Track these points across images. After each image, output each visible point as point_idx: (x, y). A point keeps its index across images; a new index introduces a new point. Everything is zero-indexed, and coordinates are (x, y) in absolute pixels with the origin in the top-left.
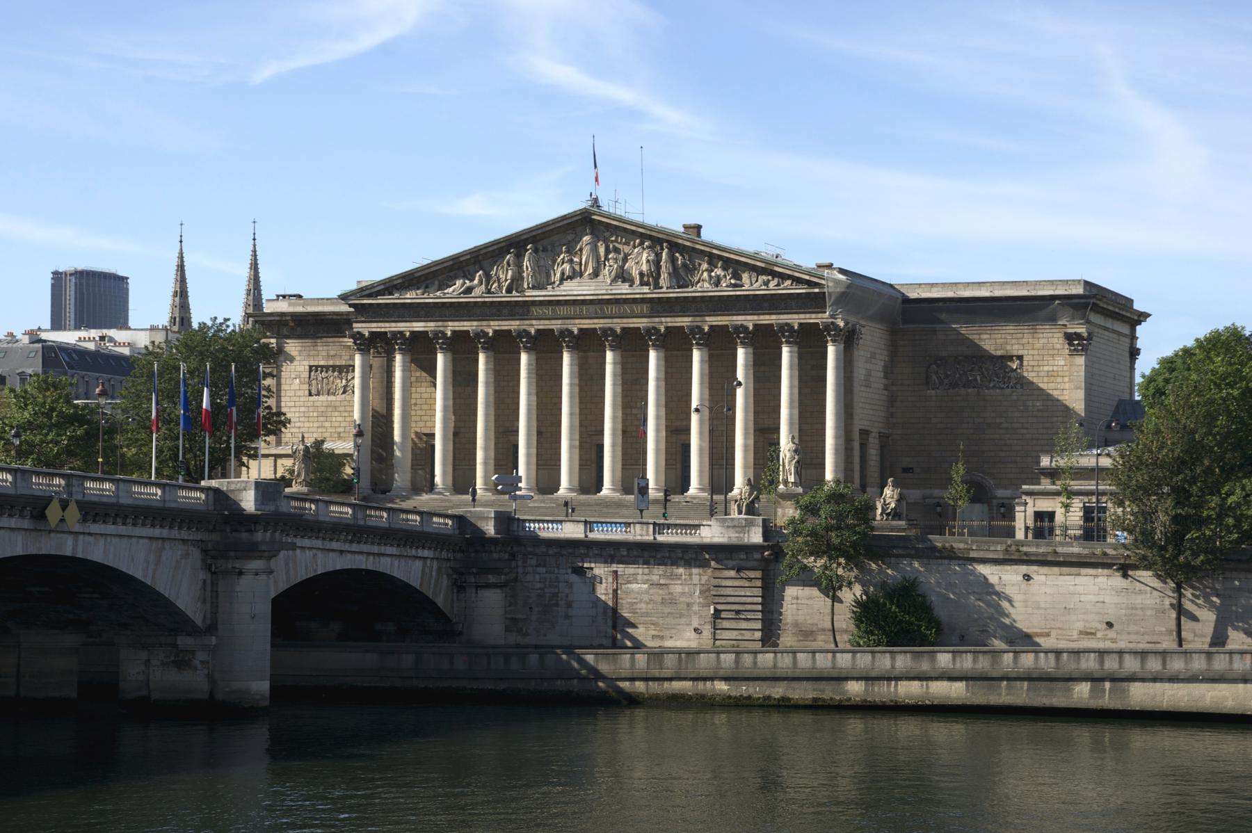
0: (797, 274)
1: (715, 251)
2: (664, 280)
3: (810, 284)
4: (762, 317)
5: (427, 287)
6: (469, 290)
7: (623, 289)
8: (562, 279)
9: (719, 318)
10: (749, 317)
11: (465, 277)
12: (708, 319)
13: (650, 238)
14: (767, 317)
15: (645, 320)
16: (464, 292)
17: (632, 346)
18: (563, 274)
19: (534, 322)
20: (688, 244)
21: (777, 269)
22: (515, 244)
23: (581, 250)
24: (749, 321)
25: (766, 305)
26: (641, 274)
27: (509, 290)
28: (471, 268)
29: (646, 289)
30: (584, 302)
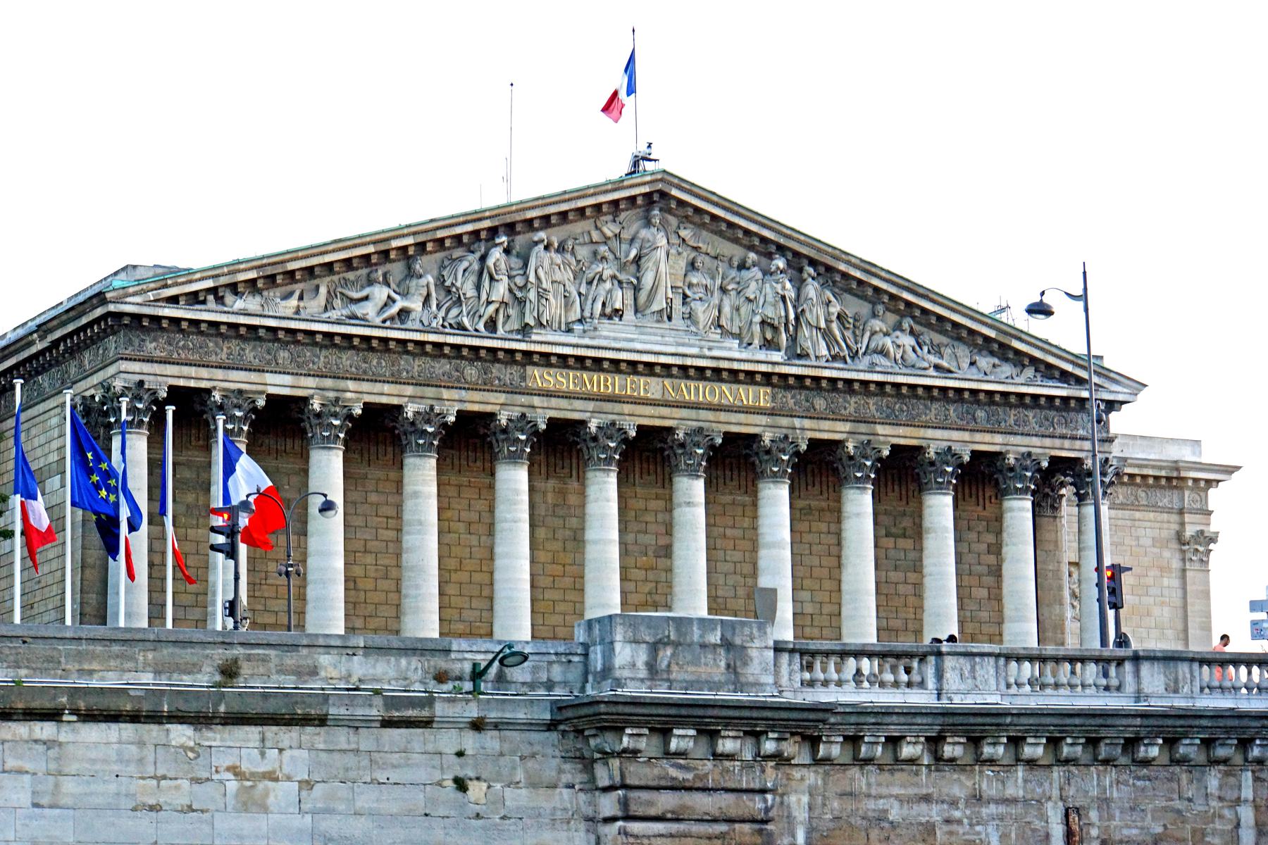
0: (1051, 360)
3: (1065, 377)
4: (978, 437)
6: (404, 313)
7: (731, 352)
8: (603, 315)
9: (901, 431)
10: (956, 435)
12: (880, 429)
13: (781, 249)
14: (987, 437)
15: (764, 420)
16: (392, 318)
18: (604, 304)
19: (536, 401)
20: (858, 274)
21: (1016, 344)
22: (510, 228)
23: (637, 260)
24: (966, 443)
25: (980, 414)
26: (763, 323)
28: (397, 269)
29: (777, 356)
30: (649, 369)
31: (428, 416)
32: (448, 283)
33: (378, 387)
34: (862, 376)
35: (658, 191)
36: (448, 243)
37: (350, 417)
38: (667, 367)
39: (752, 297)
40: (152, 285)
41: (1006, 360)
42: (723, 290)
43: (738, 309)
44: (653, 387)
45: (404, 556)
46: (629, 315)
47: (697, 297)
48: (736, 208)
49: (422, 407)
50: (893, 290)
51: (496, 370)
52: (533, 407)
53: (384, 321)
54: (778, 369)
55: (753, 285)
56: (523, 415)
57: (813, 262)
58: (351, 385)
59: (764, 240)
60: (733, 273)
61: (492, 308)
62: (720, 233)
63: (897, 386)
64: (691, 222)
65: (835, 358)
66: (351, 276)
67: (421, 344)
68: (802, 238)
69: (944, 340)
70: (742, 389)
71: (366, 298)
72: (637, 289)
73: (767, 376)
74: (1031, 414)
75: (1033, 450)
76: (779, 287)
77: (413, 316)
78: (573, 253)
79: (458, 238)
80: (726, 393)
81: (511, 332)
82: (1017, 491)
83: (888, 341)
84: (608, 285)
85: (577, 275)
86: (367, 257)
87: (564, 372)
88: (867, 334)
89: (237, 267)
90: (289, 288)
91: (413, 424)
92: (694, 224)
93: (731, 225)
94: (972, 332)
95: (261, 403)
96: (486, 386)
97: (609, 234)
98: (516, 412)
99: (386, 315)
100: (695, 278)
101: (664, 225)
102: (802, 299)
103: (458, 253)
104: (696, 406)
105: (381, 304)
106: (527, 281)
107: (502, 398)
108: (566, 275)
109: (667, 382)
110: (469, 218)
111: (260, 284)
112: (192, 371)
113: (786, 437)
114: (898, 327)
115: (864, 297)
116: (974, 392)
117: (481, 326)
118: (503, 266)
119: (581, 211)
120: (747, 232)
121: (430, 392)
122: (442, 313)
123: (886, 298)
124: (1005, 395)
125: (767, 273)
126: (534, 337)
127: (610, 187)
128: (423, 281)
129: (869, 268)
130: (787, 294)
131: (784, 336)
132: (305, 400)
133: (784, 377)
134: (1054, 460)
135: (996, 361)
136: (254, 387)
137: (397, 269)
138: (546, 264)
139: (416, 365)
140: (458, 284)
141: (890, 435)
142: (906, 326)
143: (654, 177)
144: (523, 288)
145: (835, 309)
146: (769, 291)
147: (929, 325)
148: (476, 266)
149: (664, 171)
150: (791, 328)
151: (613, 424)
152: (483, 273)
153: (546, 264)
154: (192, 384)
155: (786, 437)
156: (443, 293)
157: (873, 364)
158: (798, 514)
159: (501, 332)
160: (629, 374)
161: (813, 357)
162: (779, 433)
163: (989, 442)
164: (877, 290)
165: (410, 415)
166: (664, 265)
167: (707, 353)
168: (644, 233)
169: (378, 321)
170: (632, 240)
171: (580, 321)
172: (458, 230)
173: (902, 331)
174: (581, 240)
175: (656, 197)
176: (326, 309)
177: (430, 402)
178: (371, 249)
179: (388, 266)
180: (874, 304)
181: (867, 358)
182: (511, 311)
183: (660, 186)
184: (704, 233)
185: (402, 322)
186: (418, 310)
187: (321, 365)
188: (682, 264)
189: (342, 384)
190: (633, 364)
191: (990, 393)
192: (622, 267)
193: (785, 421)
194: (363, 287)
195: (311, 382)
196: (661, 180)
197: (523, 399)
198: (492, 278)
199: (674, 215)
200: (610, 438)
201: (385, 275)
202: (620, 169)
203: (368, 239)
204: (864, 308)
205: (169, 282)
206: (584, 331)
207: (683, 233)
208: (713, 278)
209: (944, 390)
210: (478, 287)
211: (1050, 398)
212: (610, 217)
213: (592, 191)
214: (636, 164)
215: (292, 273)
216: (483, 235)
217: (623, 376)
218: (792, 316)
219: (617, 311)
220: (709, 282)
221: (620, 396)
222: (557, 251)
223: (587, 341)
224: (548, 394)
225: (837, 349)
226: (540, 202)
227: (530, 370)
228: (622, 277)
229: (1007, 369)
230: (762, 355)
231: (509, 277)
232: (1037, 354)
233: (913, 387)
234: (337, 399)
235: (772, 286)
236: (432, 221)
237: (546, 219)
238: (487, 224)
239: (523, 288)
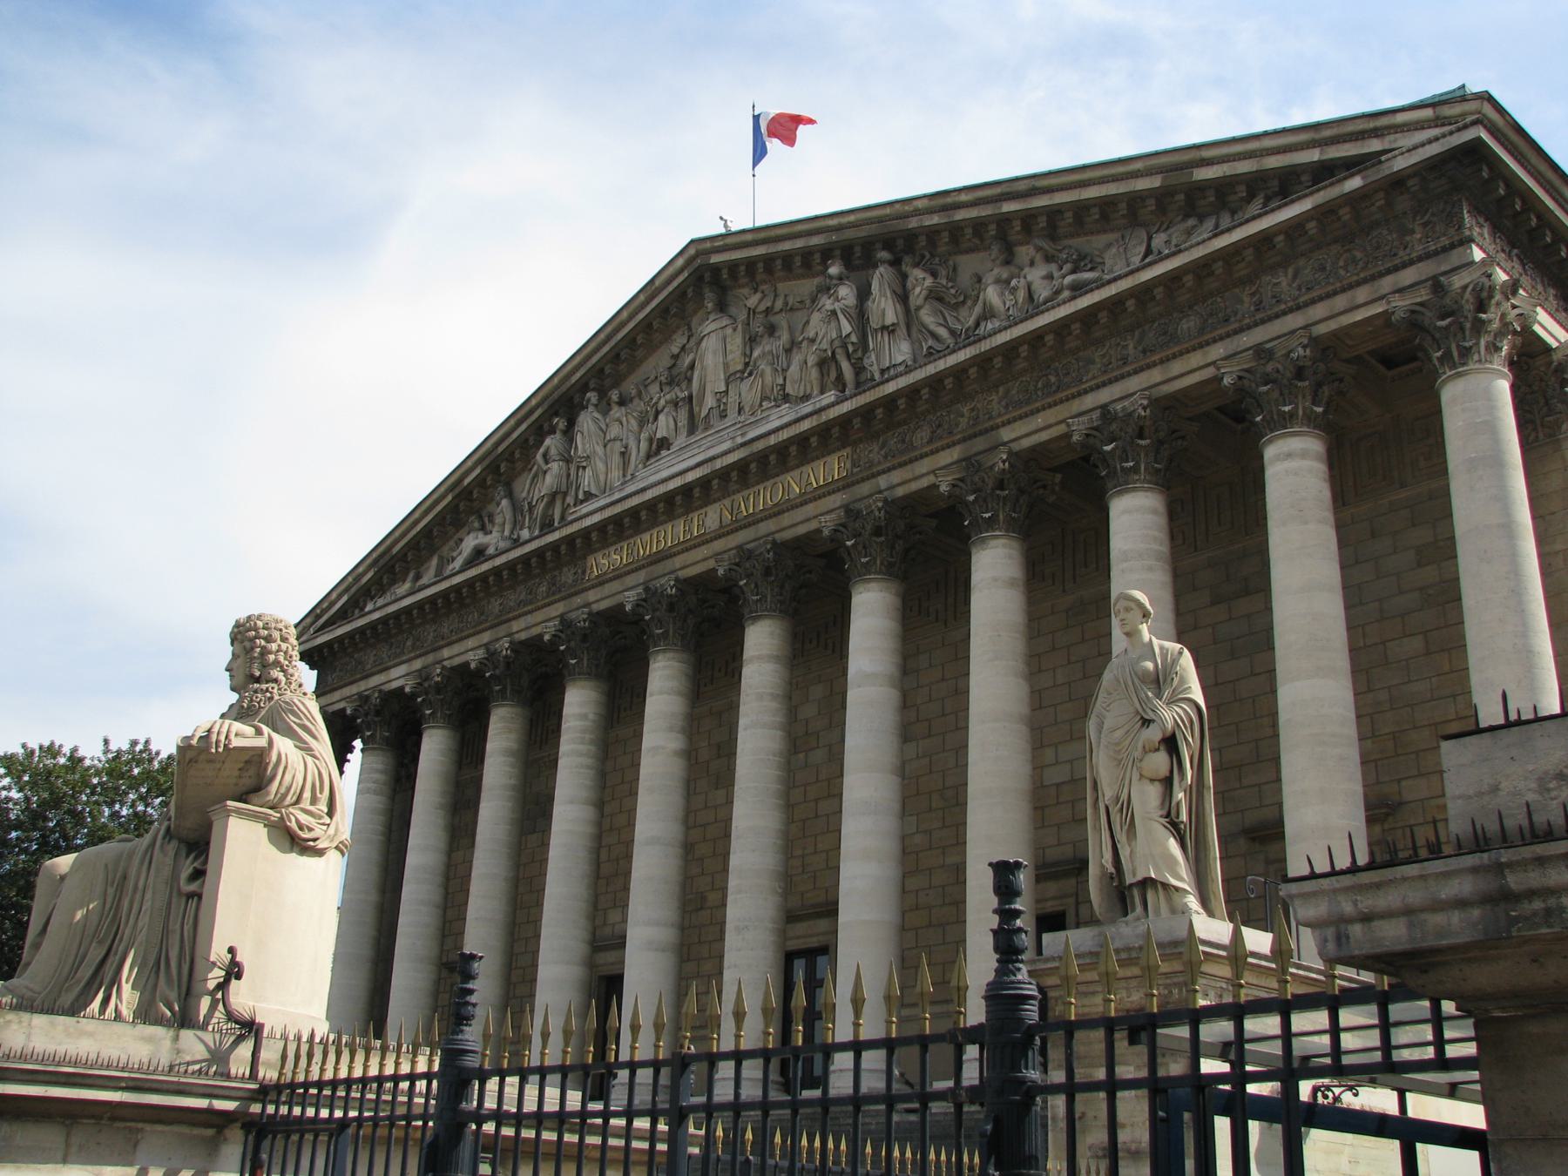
0: (1273, 162)
1: (1009, 207)
4: (1177, 367)
5: (418, 577)
6: (479, 554)
7: (777, 422)
8: (648, 457)
9: (1039, 420)
10: (1134, 383)
11: (483, 528)
12: (1006, 434)
14: (1195, 359)
18: (651, 440)
19: (591, 596)
20: (936, 219)
25: (1188, 324)
26: (822, 364)
31: (492, 655)
34: (941, 365)
37: (438, 688)
38: (704, 483)
39: (812, 335)
40: (309, 620)
54: (824, 417)
68: (852, 218)
70: (807, 469)
73: (824, 431)
74: (1283, 280)
80: (793, 483)
85: (642, 423)
86: (453, 508)
97: (675, 350)
100: (756, 354)
104: (753, 521)
110: (519, 416)
114: (1032, 264)
116: (1143, 293)
118: (553, 451)
124: (1202, 268)
129: (942, 201)
130: (837, 306)
131: (846, 366)
133: (844, 421)
135: (1191, 222)
139: (495, 606)
143: (686, 256)
150: (851, 349)
161: (877, 376)
167: (739, 440)
175: (707, 276)
178: (450, 498)
184: (780, 286)
186: (492, 541)
190: (669, 498)
193: (865, 488)
195: (418, 664)
197: (578, 600)
203: (442, 489)
207: (753, 301)
209: (1087, 317)
213: (625, 314)
218: (847, 328)
223: (617, 496)
224: (601, 581)
225: (930, 342)
226: (578, 359)
229: (1209, 224)
230: (807, 408)
232: (1244, 167)
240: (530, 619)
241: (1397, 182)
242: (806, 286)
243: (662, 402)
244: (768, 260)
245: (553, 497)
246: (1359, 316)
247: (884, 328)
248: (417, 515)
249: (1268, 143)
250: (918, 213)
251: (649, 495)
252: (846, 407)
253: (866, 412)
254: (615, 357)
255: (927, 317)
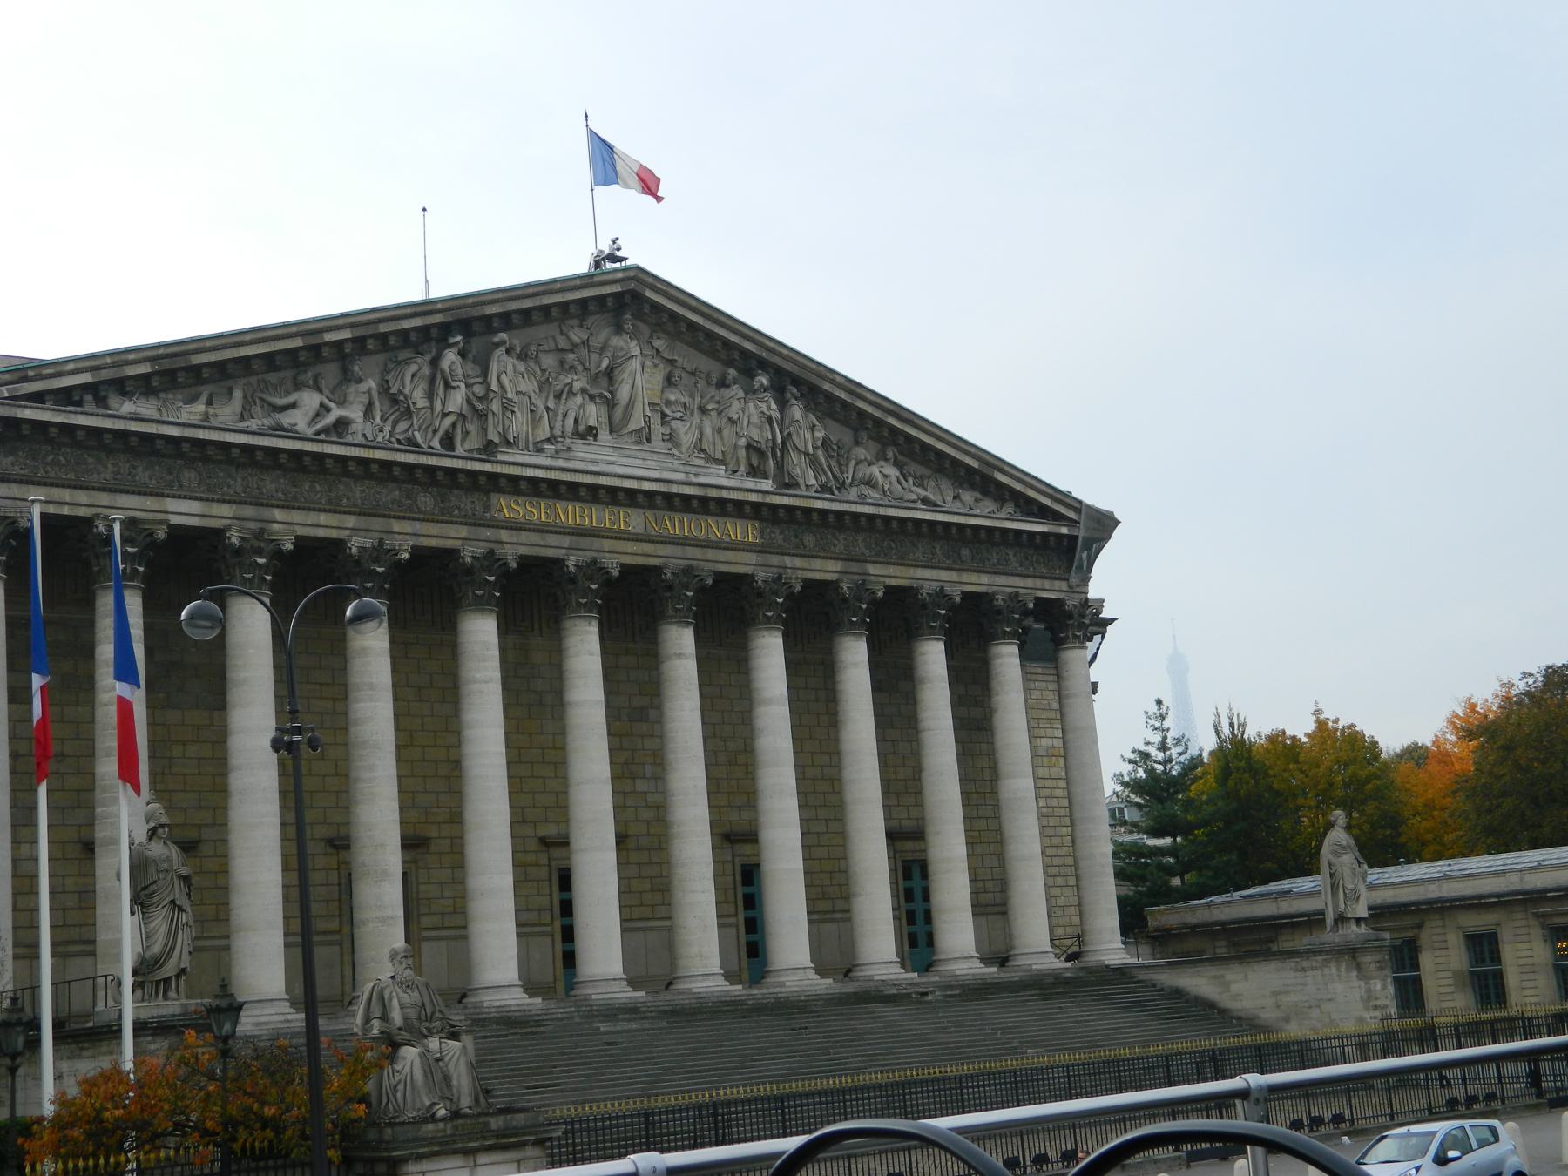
0: (1031, 493)
1: (891, 421)
2: (797, 465)
3: (1044, 513)
4: (966, 577)
6: (341, 425)
7: (718, 479)
9: (892, 570)
10: (944, 575)
12: (872, 569)
13: (763, 365)
14: (974, 578)
15: (752, 558)
16: (326, 430)
17: (726, 612)
18: (576, 421)
19: (504, 535)
20: (843, 395)
23: (610, 373)
25: (965, 552)
26: (748, 447)
27: (448, 441)
28: (331, 372)
29: (767, 485)
31: (379, 552)
32: (393, 391)
33: (312, 517)
35: (629, 291)
36: (392, 340)
37: (278, 554)
38: (650, 495)
39: (735, 417)
40: (6, 377)
41: (986, 493)
42: (703, 410)
43: (720, 431)
44: (633, 520)
45: (352, 730)
46: (604, 435)
47: (678, 415)
48: (716, 315)
49: (368, 542)
50: (878, 414)
51: (455, 498)
52: (502, 543)
53: (318, 433)
55: (736, 405)
56: (491, 552)
57: (796, 381)
58: (278, 514)
59: (745, 353)
60: (712, 391)
61: (448, 421)
62: (696, 346)
63: (887, 520)
64: (664, 331)
65: (824, 488)
66: (273, 377)
67: (365, 462)
68: (785, 352)
69: (927, 472)
71: (293, 406)
72: (611, 404)
73: (756, 506)
75: (1021, 591)
76: (764, 406)
77: (353, 427)
78: (537, 360)
79: (404, 334)
80: (714, 528)
81: (471, 451)
82: (1005, 635)
83: (875, 470)
84: (579, 399)
85: (544, 385)
87: (535, 500)
88: (853, 463)
89: (124, 357)
90: (193, 390)
91: (358, 563)
92: (668, 334)
93: (710, 335)
94: (955, 463)
95: (161, 535)
96: (444, 516)
97: (577, 340)
98: (482, 548)
99: (318, 426)
101: (635, 335)
102: (787, 421)
103: (403, 355)
105: (311, 413)
106: (488, 389)
107: (463, 532)
108: (529, 386)
109: (649, 513)
110: (418, 309)
111: (155, 383)
112: (66, 494)
113: (780, 577)
114: (881, 456)
115: (844, 422)
117: (436, 443)
119: (546, 309)
120: (727, 344)
121: (377, 523)
122: (388, 428)
123: (870, 424)
125: (750, 391)
126: (500, 457)
127: (578, 282)
128: (363, 387)
129: (854, 388)
132: (219, 533)
133: (774, 508)
134: (1039, 601)
136: (150, 516)
137: (331, 372)
138: (510, 370)
139: (357, 492)
140: (407, 391)
141: (885, 575)
142: (890, 455)
144: (484, 399)
145: (819, 434)
146: (752, 413)
147: (911, 455)
148: (426, 371)
149: (638, 268)
151: (594, 561)
152: (437, 381)
153: (510, 370)
154: (66, 511)
155: (780, 577)
156: (387, 404)
157: (862, 496)
158: (792, 666)
159: (459, 451)
160: (607, 504)
162: (771, 574)
163: (977, 582)
164: (862, 414)
165: (354, 550)
166: (640, 380)
167: (694, 479)
168: (616, 341)
169: (310, 432)
170: (603, 349)
171: (549, 440)
172: (406, 324)
173: (886, 460)
174: (545, 347)
175: (627, 299)
176: (242, 418)
177: (377, 535)
178: (298, 343)
179: (320, 368)
180: (856, 430)
181: (853, 493)
182: (470, 427)
183: (633, 285)
185: (340, 435)
186: (356, 420)
187: (239, 489)
188: (659, 377)
189: (266, 513)
190: (613, 491)
191: (976, 528)
192: (594, 380)
193: (775, 560)
194: (288, 393)
195: (226, 510)
196: (634, 278)
197: (488, 533)
198: (447, 386)
199: (645, 322)
200: (591, 579)
201: (316, 378)
202: (580, 265)
203: (294, 329)
204: (847, 436)
205: (31, 373)
206: (557, 452)
207: (657, 343)
208: (692, 396)
210: (430, 395)
211: (1032, 534)
212: (575, 322)
213: (558, 286)
214: (597, 264)
215: (198, 368)
216: (434, 333)
217: (600, 507)
218: (779, 440)
219: (591, 428)
220: (687, 400)
221: (600, 530)
222: (519, 357)
223: (560, 463)
227: (494, 497)
228: (593, 391)
229: (988, 506)
231: (467, 386)
232: (1018, 487)
233: (902, 521)
234: (262, 531)
235: (756, 406)
236: (374, 310)
237: (506, 316)
238: (438, 319)
239: (484, 399)
240: (418, 527)
241: (1073, 539)
242: (705, 363)
243: (577, 385)
244: (692, 325)
245: (461, 415)
246: (1045, 595)
247: (807, 454)
248: (248, 338)
249: (1034, 482)
250: (832, 382)
251: (603, 481)
252: (785, 501)
253: (790, 509)
254: (526, 313)
255: (820, 453)
